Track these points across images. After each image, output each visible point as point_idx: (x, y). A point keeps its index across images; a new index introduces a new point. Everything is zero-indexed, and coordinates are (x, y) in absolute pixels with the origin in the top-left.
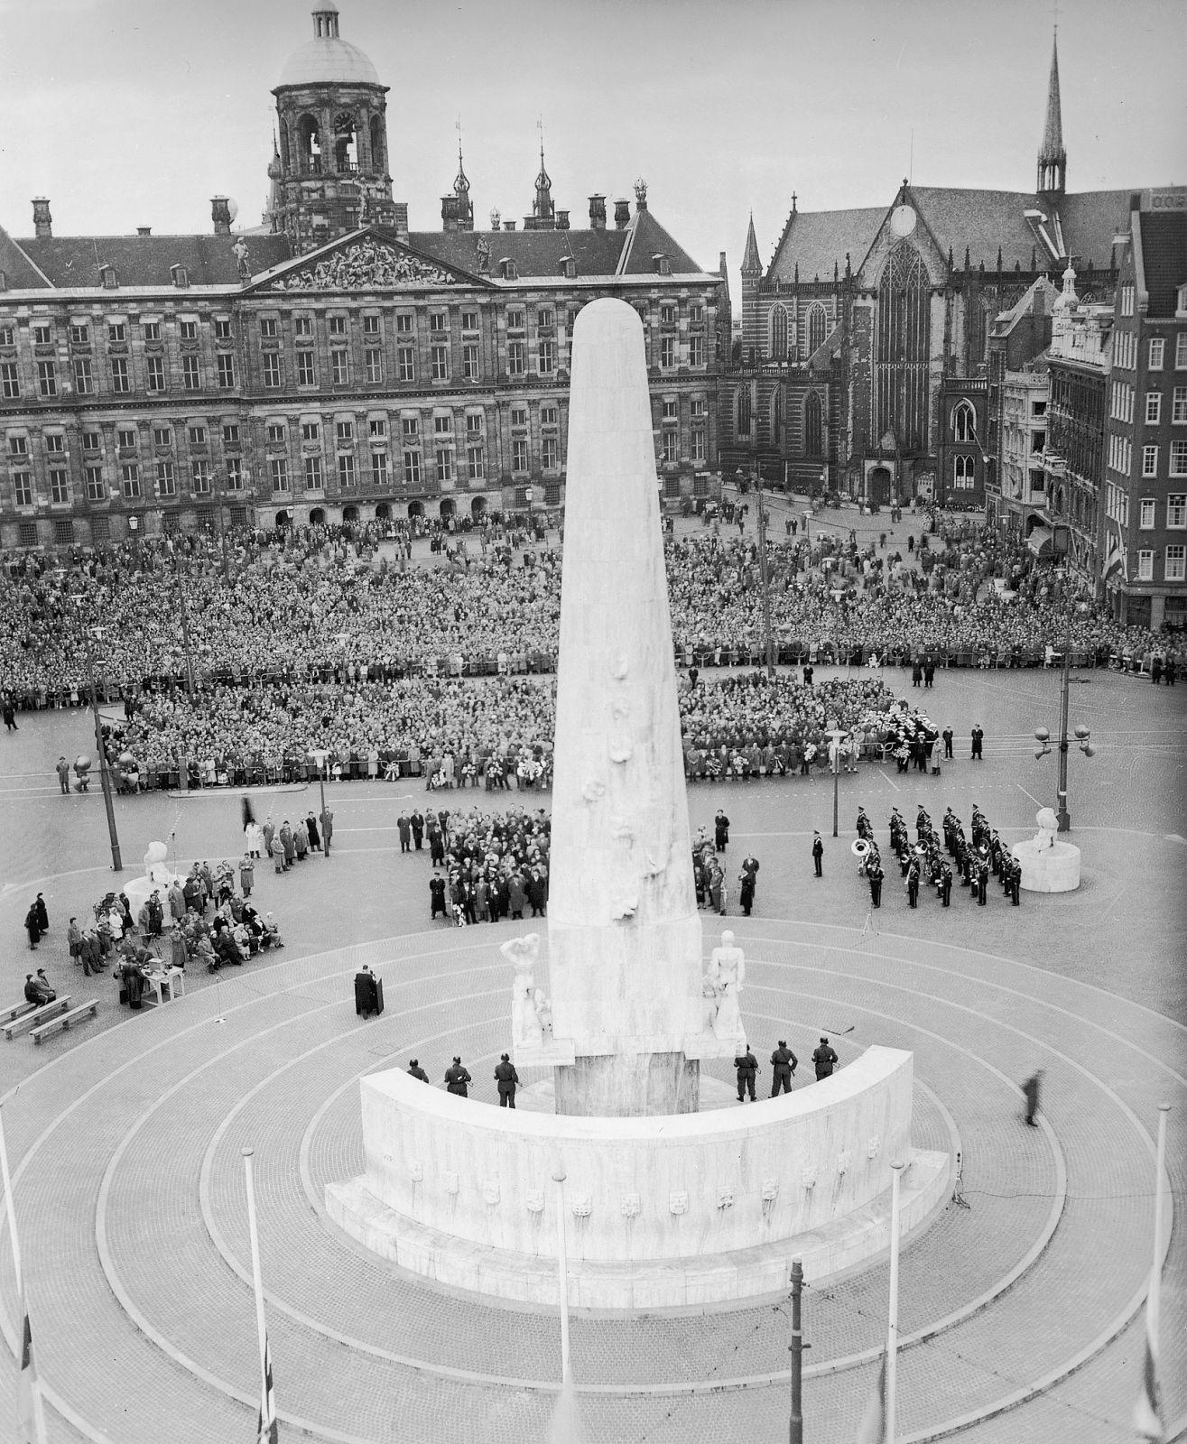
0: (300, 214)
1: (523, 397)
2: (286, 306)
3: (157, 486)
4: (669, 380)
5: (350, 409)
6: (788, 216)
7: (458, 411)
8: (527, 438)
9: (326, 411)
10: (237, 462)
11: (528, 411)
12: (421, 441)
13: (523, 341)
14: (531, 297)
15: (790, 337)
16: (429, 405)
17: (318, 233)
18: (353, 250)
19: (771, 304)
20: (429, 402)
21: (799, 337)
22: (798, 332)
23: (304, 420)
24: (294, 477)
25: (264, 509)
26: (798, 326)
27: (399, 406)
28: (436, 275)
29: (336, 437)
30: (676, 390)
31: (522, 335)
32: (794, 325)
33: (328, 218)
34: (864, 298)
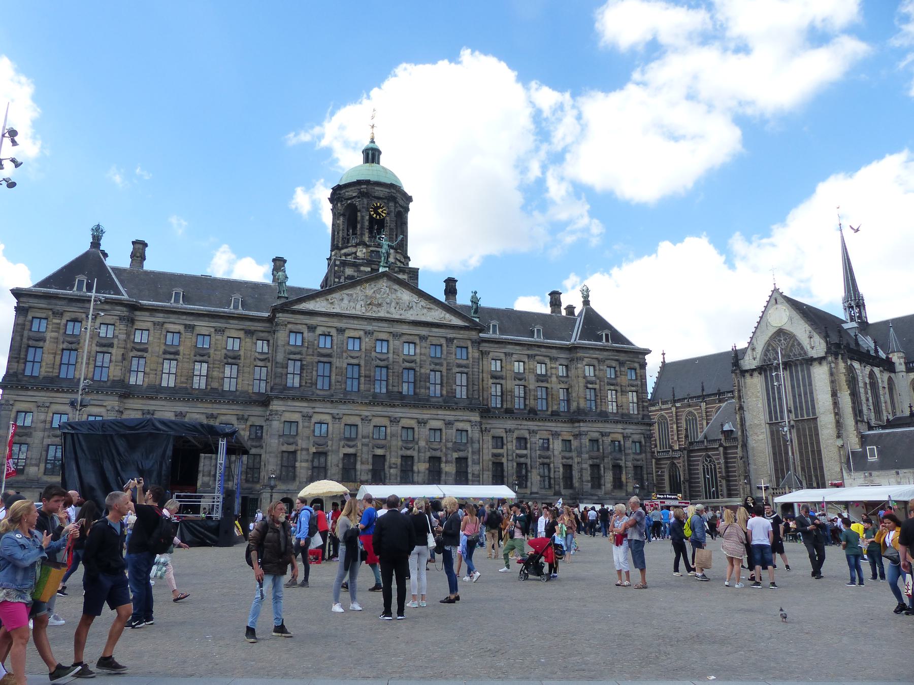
1: (501, 426)
5: (357, 412)
6: (661, 365)
7: (449, 424)
8: (504, 460)
9: (335, 411)
13: (503, 382)
14: (509, 349)
15: (672, 435)
16: (426, 417)
19: (656, 415)
21: (678, 435)
22: (678, 431)
23: (316, 418)
26: (677, 427)
27: (400, 415)
30: (620, 431)
32: (675, 426)
34: (751, 375)
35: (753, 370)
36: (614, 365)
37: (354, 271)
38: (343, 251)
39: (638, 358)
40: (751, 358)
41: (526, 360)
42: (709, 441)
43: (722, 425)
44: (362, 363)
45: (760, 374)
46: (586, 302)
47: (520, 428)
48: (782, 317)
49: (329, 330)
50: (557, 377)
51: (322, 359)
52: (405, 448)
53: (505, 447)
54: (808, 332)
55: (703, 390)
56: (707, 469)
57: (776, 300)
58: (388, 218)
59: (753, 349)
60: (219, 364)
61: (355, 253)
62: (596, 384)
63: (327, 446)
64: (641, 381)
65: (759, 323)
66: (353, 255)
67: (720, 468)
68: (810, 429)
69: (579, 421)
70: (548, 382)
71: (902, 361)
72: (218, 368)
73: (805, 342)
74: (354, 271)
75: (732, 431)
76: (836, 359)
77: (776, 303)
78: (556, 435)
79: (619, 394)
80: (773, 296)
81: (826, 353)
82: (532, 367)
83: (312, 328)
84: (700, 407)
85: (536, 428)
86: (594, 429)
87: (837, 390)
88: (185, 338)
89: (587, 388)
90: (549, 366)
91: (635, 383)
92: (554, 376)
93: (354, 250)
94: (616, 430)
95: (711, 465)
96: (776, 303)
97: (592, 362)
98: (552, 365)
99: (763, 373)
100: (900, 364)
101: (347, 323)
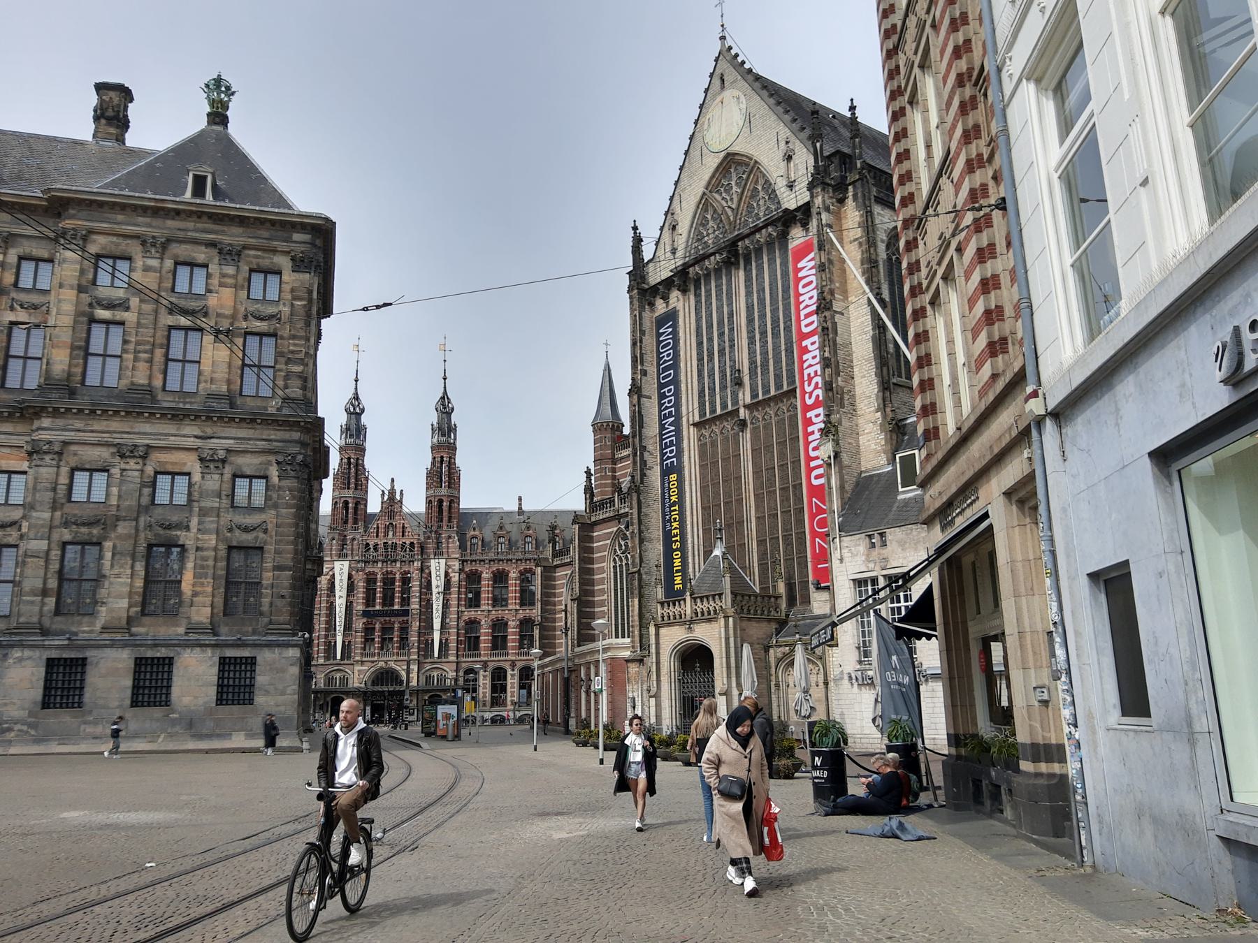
30: (191, 442)
36: (200, 255)
39: (288, 240)
40: (668, 248)
45: (684, 291)
54: (782, 144)
59: (674, 228)
62: (127, 309)
64: (292, 305)
68: (780, 423)
76: (842, 201)
80: (718, 72)
87: (832, 292)
89: (93, 320)
91: (271, 310)
94: (172, 441)
95: (627, 559)
97: (123, 247)
99: (692, 288)
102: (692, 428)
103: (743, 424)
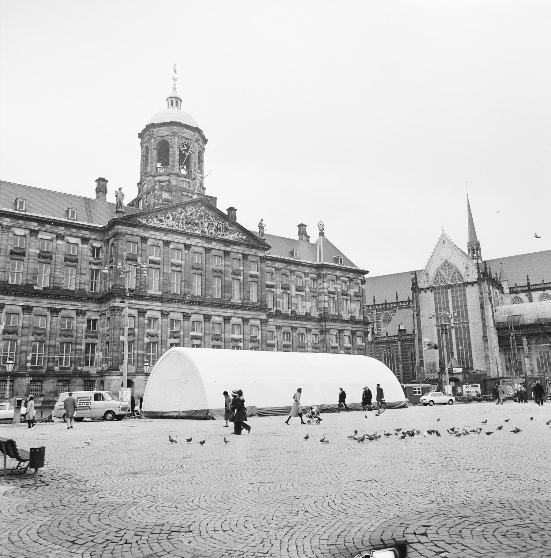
0: (156, 189)
1: (274, 323)
2: (145, 234)
3: (29, 358)
4: (347, 322)
10: (94, 345)
11: (276, 332)
12: (223, 339)
13: (274, 290)
17: (165, 203)
18: (191, 208)
20: (229, 312)
24: (138, 355)
25: (114, 377)
28: (236, 234)
29: (169, 329)
30: (350, 328)
31: (273, 286)
33: (172, 196)
34: (425, 292)
35: (428, 288)
37: (169, 196)
38: (157, 178)
40: (425, 280)
41: (289, 274)
42: (388, 337)
43: (399, 326)
44: (183, 270)
45: (431, 291)
46: (322, 234)
47: (286, 325)
48: (446, 253)
49: (157, 241)
50: (309, 288)
51: (152, 265)
52: (215, 339)
53: (276, 339)
55: (374, 301)
56: (388, 356)
57: (444, 241)
58: (193, 155)
59: (427, 274)
60: (60, 266)
61: (169, 181)
62: (335, 294)
63: (158, 337)
65: (432, 257)
66: (167, 183)
67: (397, 355)
69: (325, 321)
70: (303, 292)
71: (508, 287)
72: (60, 269)
73: (463, 271)
74: (169, 196)
75: (405, 330)
76: (483, 283)
77: (444, 243)
78: (308, 330)
79: (349, 302)
81: (478, 279)
82: (293, 279)
83: (144, 240)
84: (373, 313)
85: (296, 326)
86: (334, 327)
88: (30, 241)
90: (304, 279)
92: (307, 287)
93: (167, 178)
95: (390, 354)
96: (444, 243)
98: (307, 279)
100: (507, 288)
101: (171, 237)
102: (436, 327)
103: (453, 327)
